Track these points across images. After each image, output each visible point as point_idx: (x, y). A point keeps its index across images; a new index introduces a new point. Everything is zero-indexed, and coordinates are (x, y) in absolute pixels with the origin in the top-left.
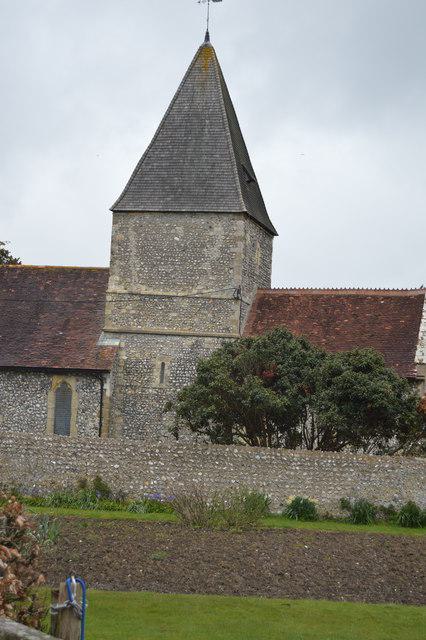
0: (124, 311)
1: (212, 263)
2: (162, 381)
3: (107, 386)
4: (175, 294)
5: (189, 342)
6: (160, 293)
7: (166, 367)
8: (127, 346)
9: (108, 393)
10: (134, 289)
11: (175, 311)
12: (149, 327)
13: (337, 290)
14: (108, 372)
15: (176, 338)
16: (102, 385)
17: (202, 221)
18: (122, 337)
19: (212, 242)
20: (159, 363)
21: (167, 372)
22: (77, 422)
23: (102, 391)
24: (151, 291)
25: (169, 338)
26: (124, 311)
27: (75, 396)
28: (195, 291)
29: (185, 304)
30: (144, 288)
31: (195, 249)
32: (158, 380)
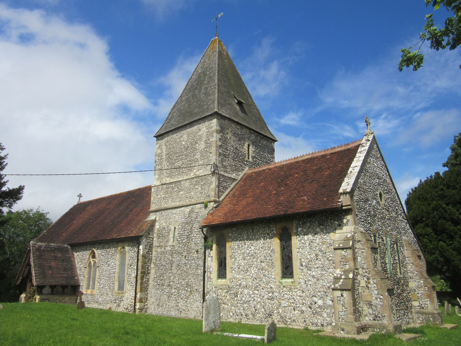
0: (159, 196)
1: (201, 152)
2: (174, 241)
3: (141, 247)
4: (182, 179)
5: (188, 209)
6: (175, 180)
7: (176, 229)
8: (159, 219)
9: (141, 252)
10: (164, 181)
11: (183, 190)
12: (171, 204)
13: (298, 158)
14: (142, 236)
15: (182, 209)
16: (139, 247)
17: (195, 128)
18: (158, 213)
19: (200, 139)
20: (173, 228)
21: (176, 233)
22: (128, 274)
23: (139, 249)
24: (172, 180)
25: (179, 209)
26: (159, 196)
27: (127, 255)
28: (192, 174)
29: (187, 184)
30: (168, 179)
31: (191, 147)
32: (172, 240)
